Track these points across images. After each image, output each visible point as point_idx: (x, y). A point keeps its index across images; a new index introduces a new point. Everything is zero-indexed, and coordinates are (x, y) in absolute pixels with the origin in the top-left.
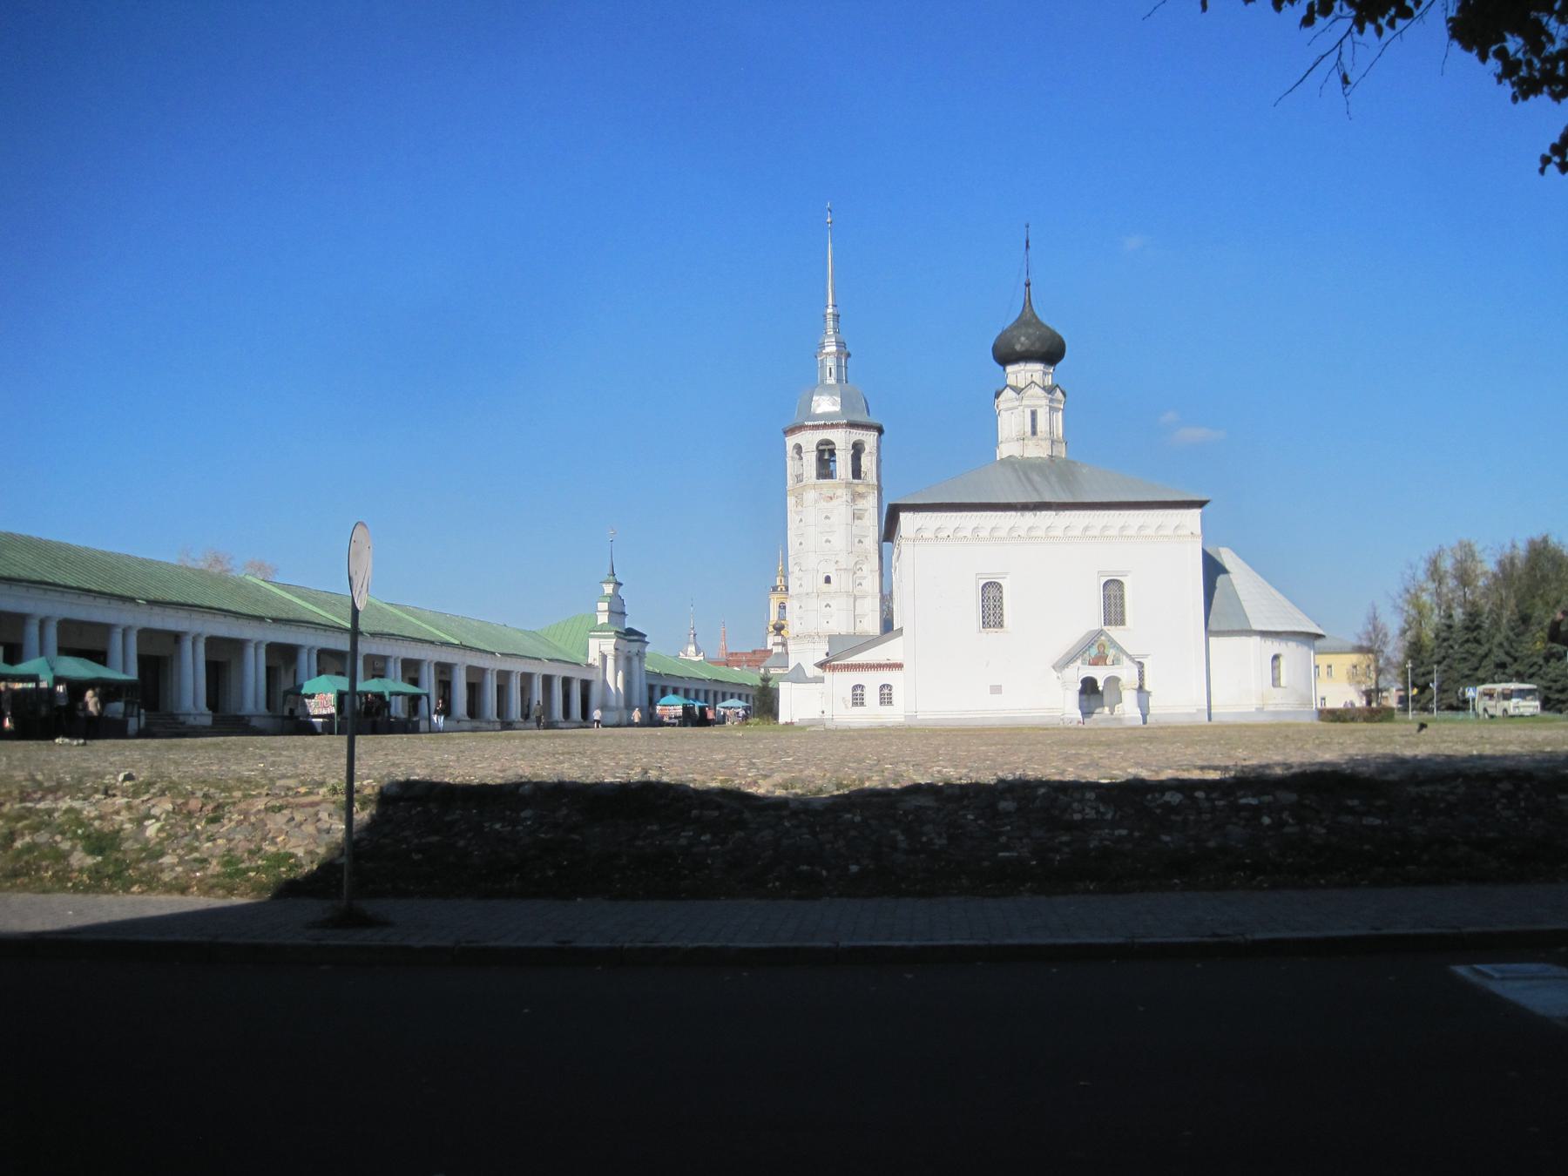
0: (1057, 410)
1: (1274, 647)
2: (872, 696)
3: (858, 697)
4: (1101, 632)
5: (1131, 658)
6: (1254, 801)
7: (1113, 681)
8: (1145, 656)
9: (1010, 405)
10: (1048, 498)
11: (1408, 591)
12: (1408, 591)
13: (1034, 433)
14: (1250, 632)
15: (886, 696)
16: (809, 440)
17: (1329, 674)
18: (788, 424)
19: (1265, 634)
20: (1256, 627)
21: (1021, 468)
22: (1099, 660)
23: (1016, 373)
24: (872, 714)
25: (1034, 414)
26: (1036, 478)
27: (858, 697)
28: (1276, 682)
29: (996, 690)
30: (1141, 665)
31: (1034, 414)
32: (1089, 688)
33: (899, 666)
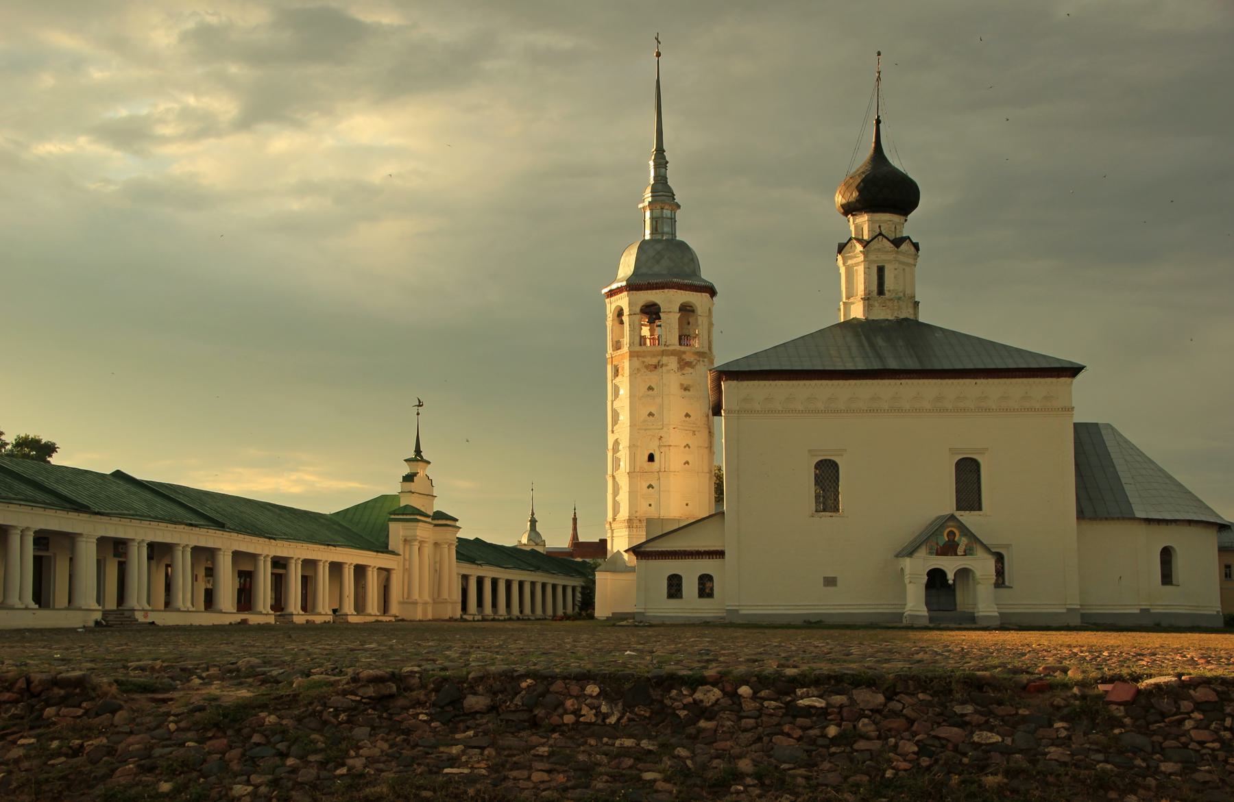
1: (1165, 537)
2: (690, 587)
4: (952, 517)
5: (987, 548)
6: (819, 703)
7: (964, 573)
10: (893, 364)
13: (881, 292)
14: (1134, 519)
15: (705, 586)
19: (1149, 521)
20: (1140, 514)
22: (949, 549)
24: (690, 605)
25: (881, 270)
26: (880, 342)
28: (1167, 578)
30: (1000, 558)
31: (881, 270)
32: (936, 579)
33: (720, 554)
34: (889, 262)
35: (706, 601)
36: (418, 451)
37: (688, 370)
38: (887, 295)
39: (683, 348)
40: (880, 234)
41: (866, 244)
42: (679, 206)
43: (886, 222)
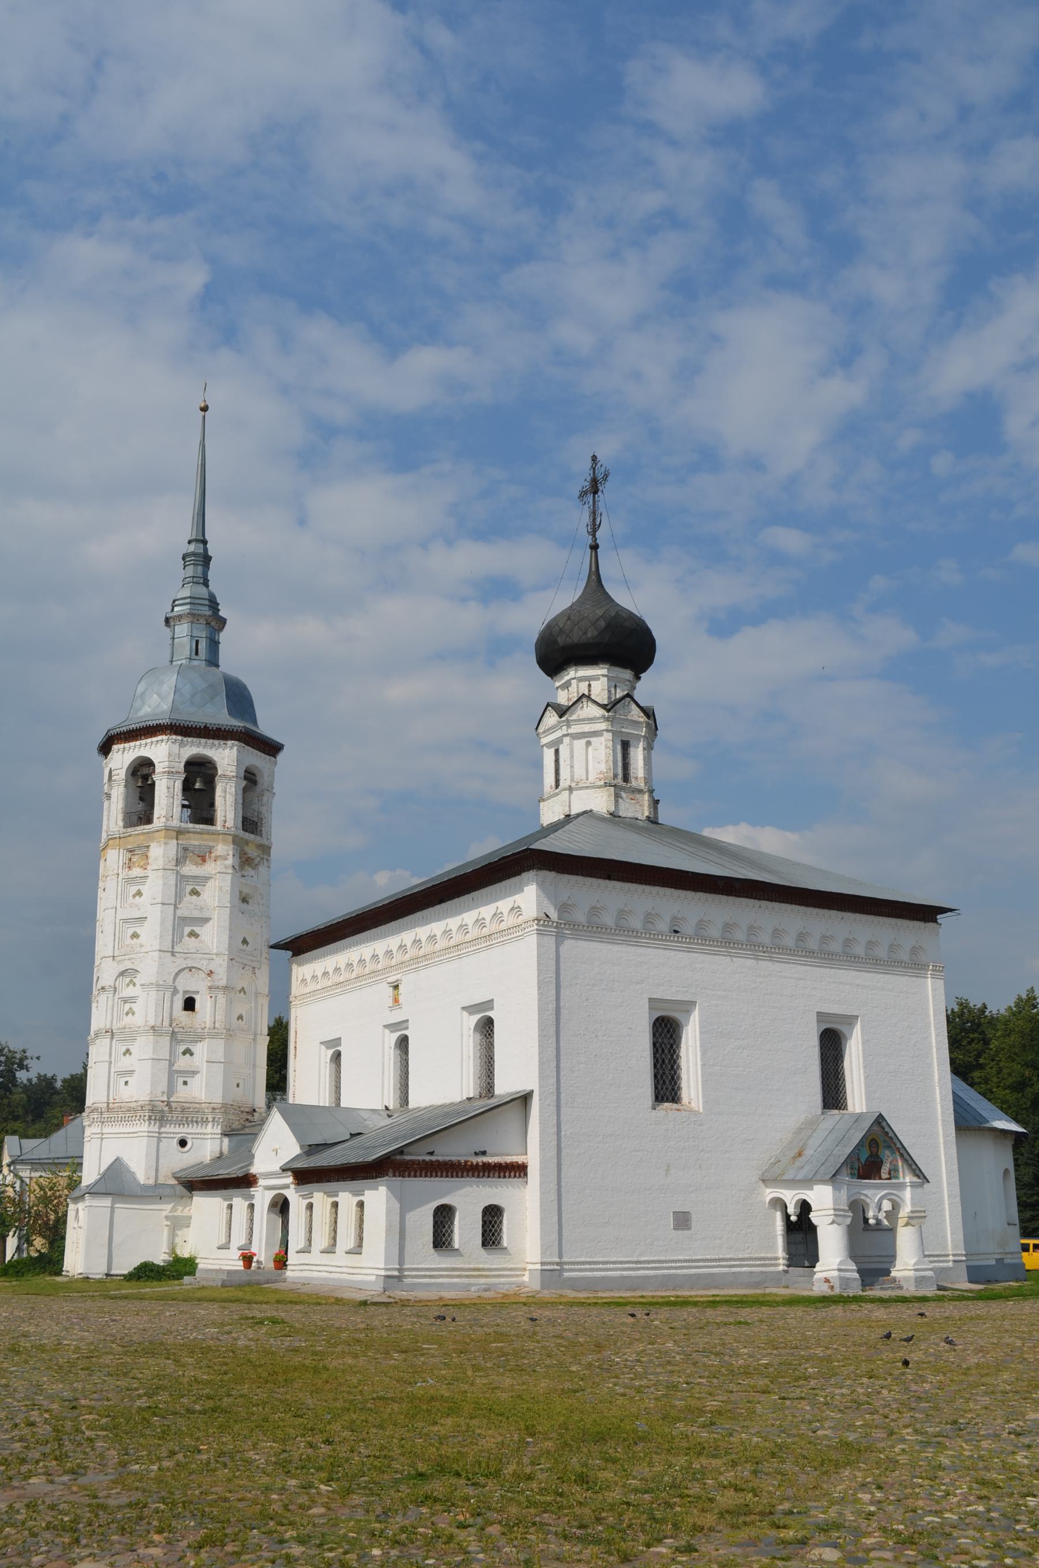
2: (466, 1229)
3: (441, 1239)
9: (587, 728)
13: (626, 778)
16: (164, 754)
23: (589, 679)
25: (625, 746)
27: (441, 1239)
31: (625, 746)
33: (519, 1170)
37: (249, 871)
38: (634, 783)
39: (248, 836)
40: (628, 695)
41: (610, 707)
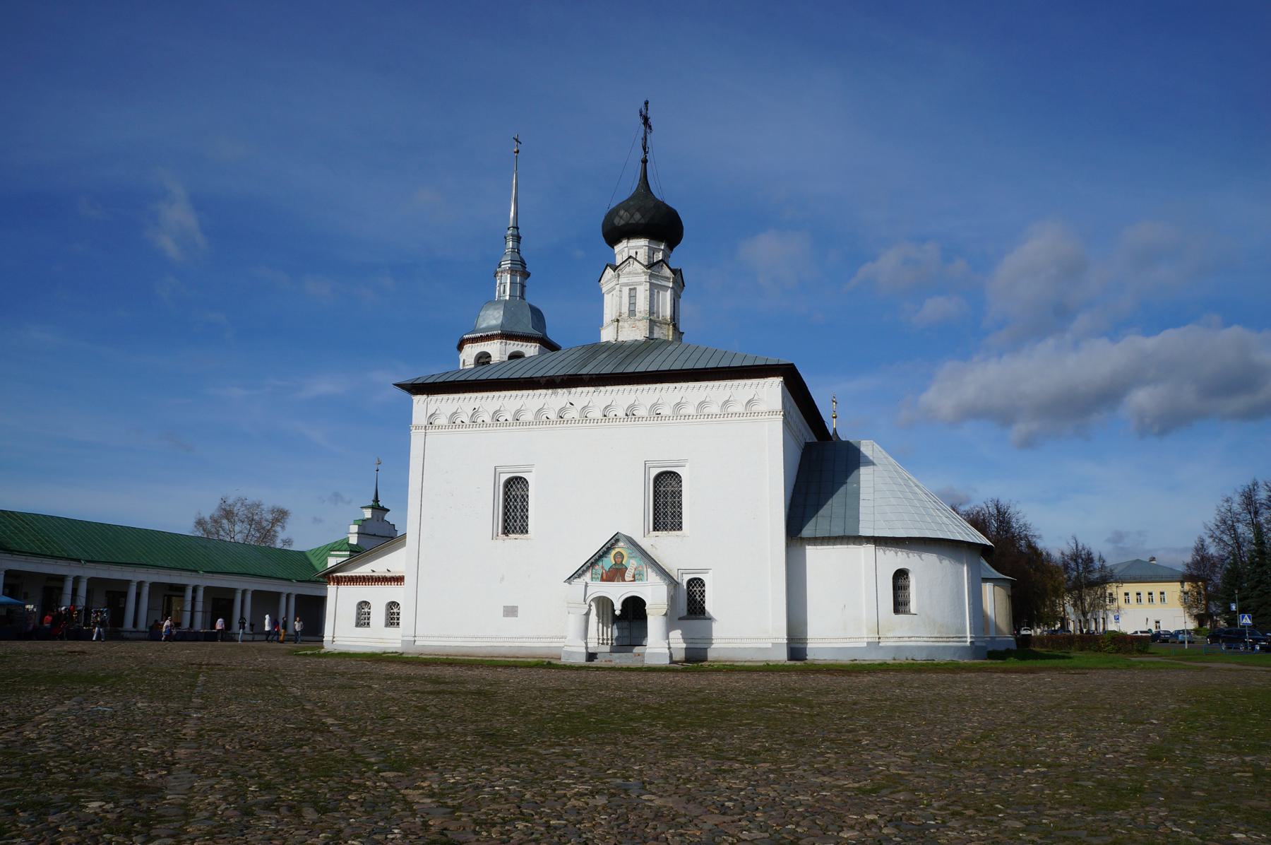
0: (665, 288)
1: (895, 559)
2: (378, 615)
3: (363, 618)
8: (706, 571)
9: (610, 286)
11: (1225, 523)
12: (1225, 523)
13: (632, 312)
17: (1163, 600)
18: (457, 343)
20: (864, 531)
21: (617, 348)
22: (616, 574)
27: (363, 618)
28: (900, 605)
29: (511, 611)
34: (640, 284)
35: (392, 630)
36: (376, 500)
42: (529, 275)
43: (641, 247)
